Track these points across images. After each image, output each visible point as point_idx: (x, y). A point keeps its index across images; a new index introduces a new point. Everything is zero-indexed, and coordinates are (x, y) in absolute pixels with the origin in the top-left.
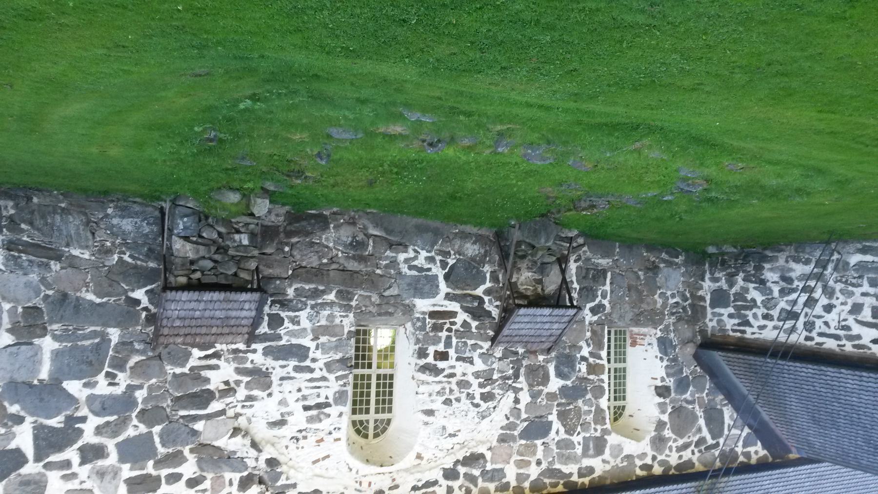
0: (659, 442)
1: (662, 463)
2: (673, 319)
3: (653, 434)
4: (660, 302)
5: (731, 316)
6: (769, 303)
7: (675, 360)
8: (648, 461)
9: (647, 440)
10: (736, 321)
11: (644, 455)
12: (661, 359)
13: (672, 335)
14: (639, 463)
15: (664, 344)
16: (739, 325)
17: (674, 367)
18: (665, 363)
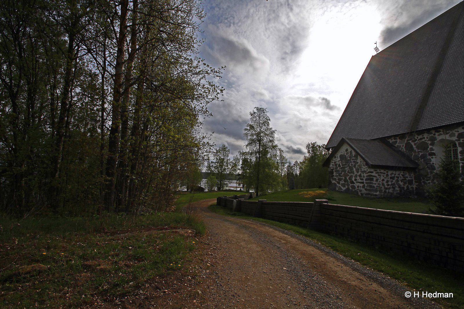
0: (433, 139)
1: (431, 133)
2: (429, 176)
3: (436, 141)
4: (435, 181)
5: (407, 177)
6: (397, 181)
7: (427, 164)
8: (437, 134)
9: (438, 140)
10: (406, 176)
11: (438, 135)
12: (433, 164)
13: (429, 171)
14: (442, 133)
15: (433, 168)
16: (405, 175)
17: (427, 162)
18: (431, 162)
